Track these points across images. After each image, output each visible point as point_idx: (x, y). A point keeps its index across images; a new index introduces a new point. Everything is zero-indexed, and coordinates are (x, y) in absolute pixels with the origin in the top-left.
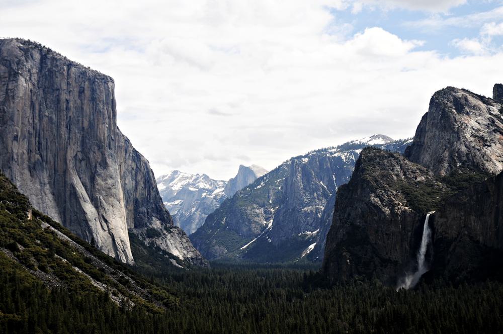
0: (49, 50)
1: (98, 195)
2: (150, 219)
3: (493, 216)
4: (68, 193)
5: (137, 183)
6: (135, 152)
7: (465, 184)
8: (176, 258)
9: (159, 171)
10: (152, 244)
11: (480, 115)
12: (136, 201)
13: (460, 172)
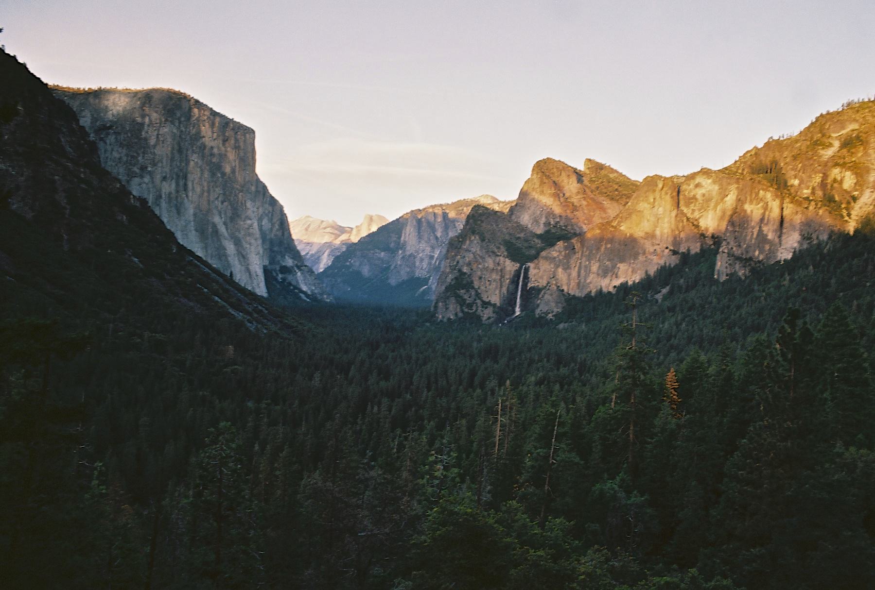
0: (197, 101)
1: (237, 234)
2: (283, 256)
3: (577, 268)
4: (210, 230)
5: (273, 225)
8: (305, 293)
9: (292, 217)
10: (284, 279)
13: (553, 231)
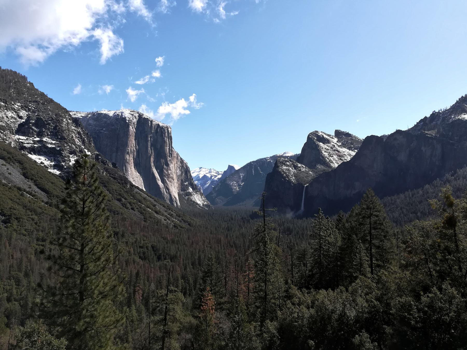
0: (143, 115)
6: (181, 159)
7: (322, 173)
8: (198, 204)
11: (329, 143)
12: (182, 180)
